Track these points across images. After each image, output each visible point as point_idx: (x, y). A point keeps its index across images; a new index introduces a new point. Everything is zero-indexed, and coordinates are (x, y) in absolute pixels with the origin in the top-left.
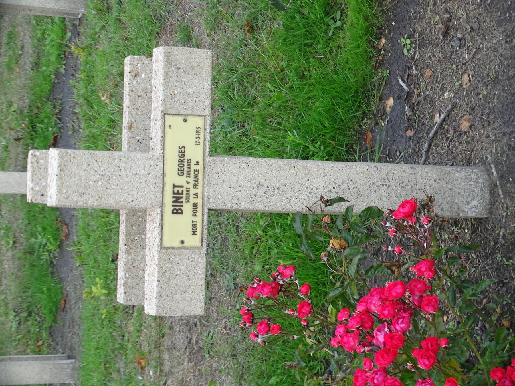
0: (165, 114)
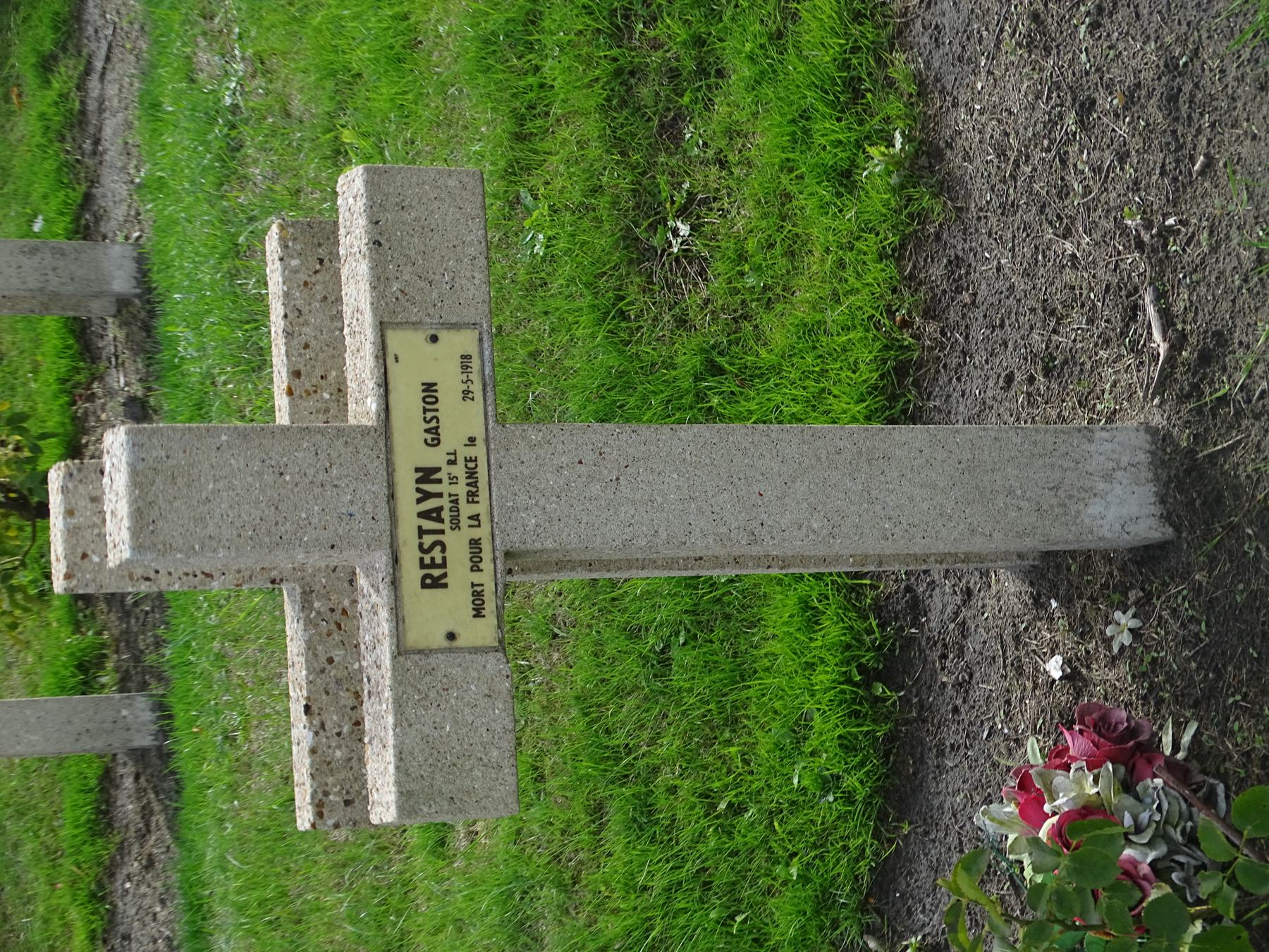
0: (382, 328)
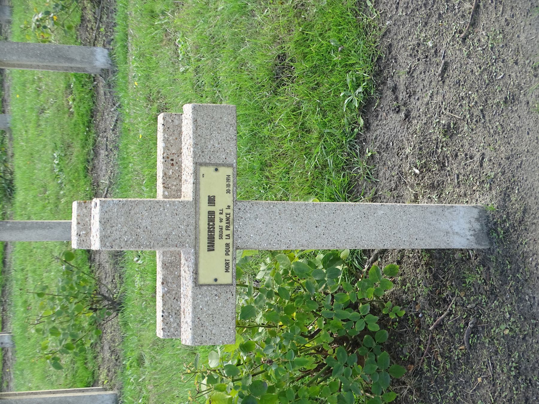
0: (198, 165)
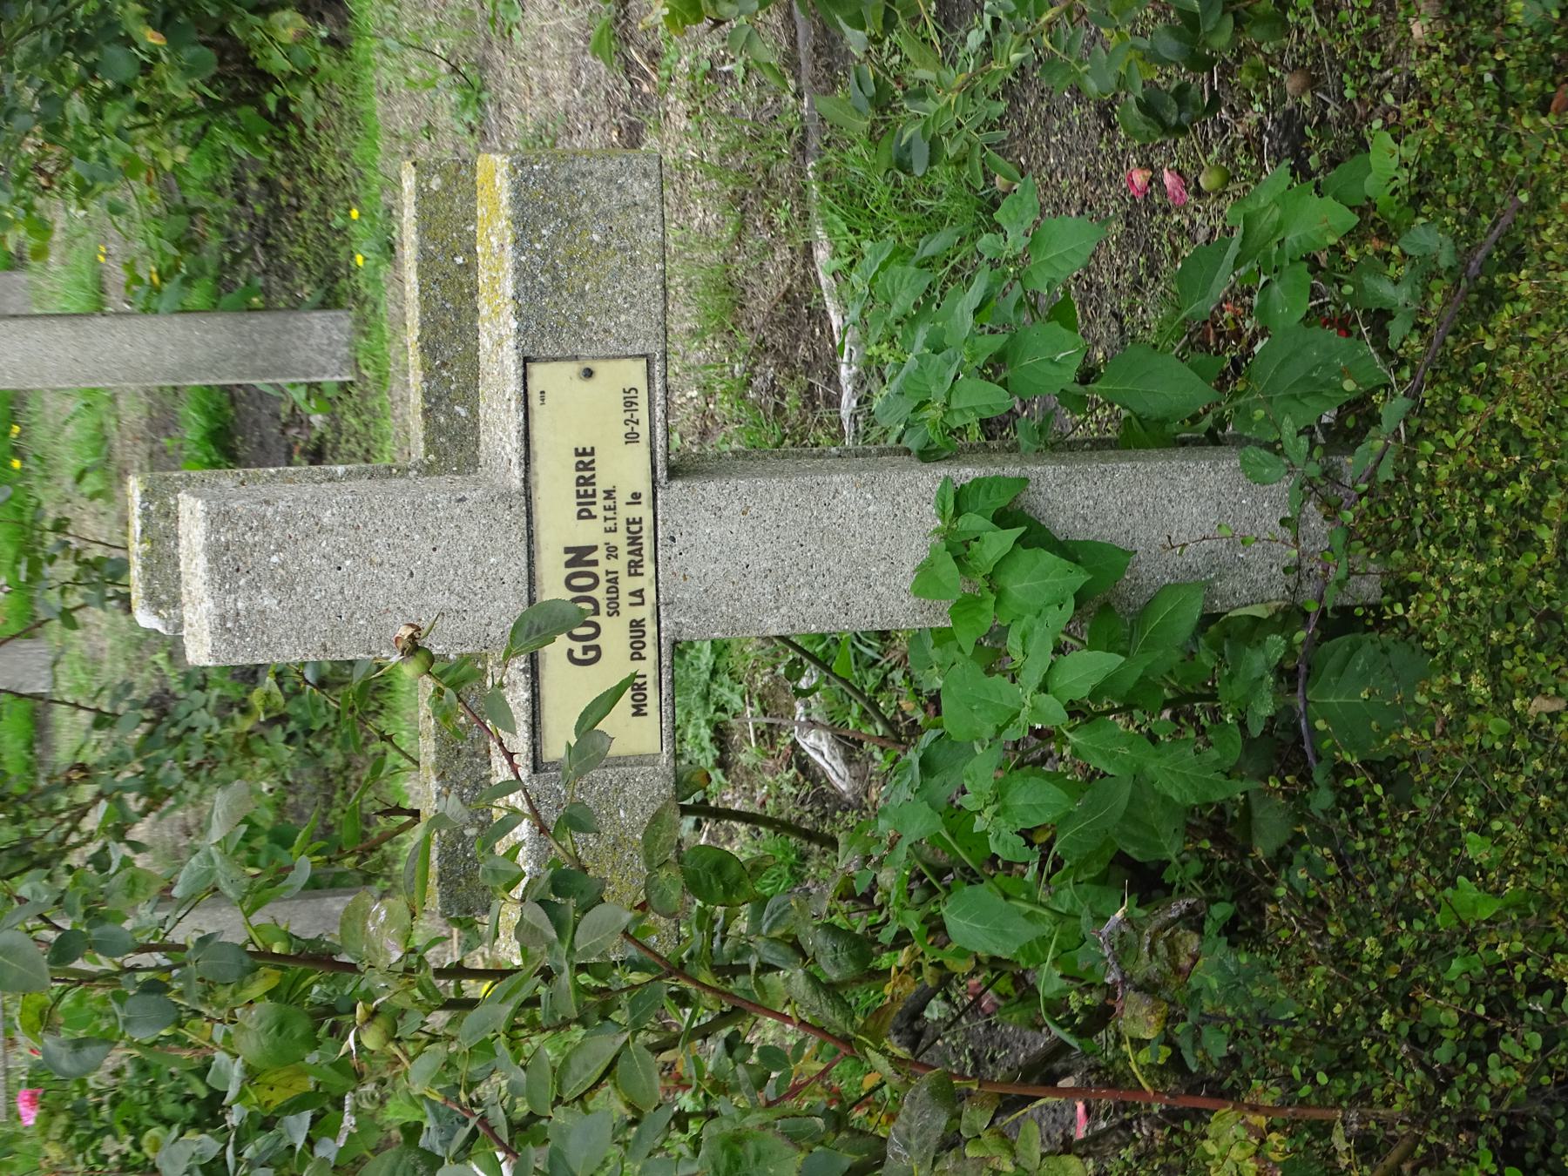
0: (526, 361)
